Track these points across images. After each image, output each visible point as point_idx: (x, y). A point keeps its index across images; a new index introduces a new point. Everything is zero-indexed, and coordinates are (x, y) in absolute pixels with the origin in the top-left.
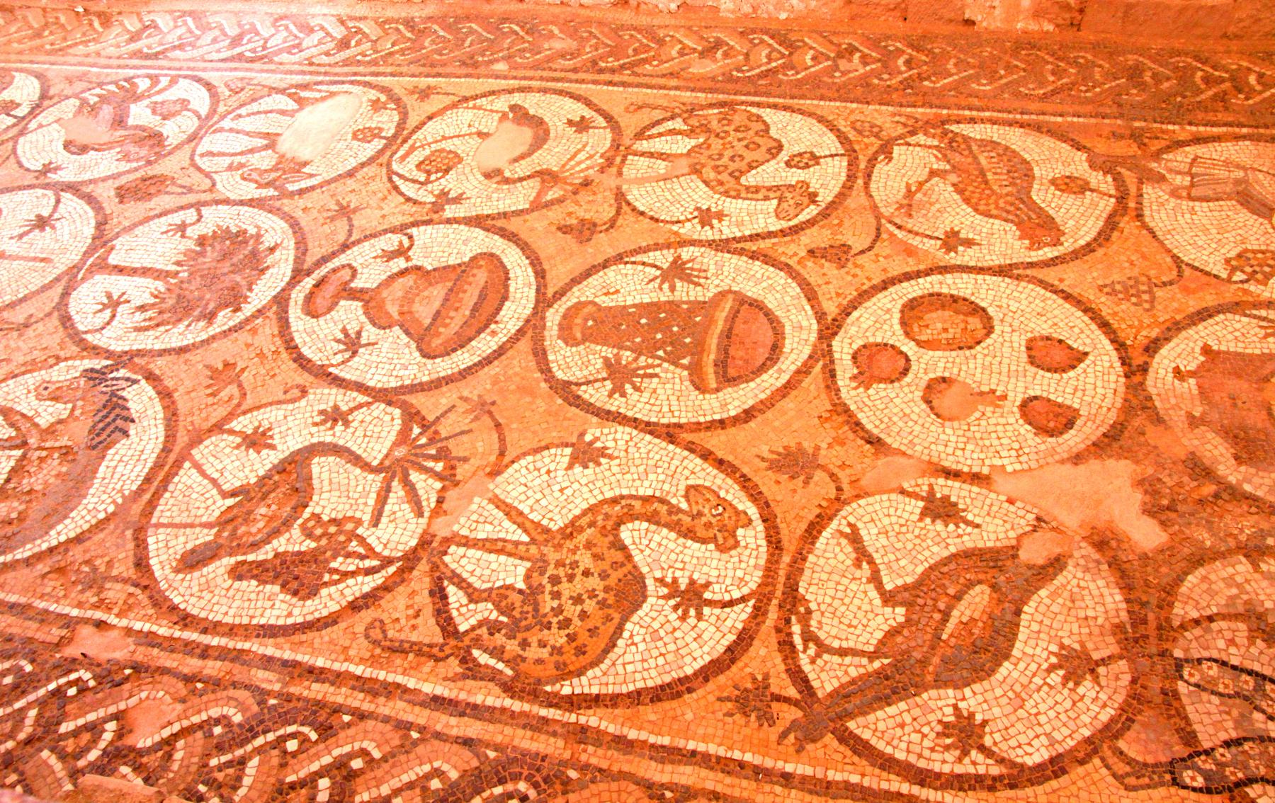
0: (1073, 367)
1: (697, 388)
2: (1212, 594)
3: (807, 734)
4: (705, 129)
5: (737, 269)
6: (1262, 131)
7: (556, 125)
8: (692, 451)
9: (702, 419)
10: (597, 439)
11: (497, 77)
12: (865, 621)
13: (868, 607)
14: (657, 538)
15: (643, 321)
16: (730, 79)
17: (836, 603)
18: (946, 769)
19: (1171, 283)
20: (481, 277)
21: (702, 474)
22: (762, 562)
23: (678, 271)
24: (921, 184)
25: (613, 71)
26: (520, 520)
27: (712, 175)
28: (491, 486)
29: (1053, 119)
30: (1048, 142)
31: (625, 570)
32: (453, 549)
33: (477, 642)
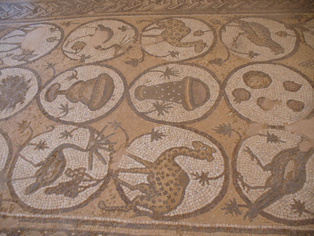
1: (186, 109)
8: (191, 130)
9: (191, 119)
10: (158, 130)
12: (260, 177)
15: (162, 90)
17: (249, 173)
21: (196, 137)
22: (223, 163)
26: (140, 161)
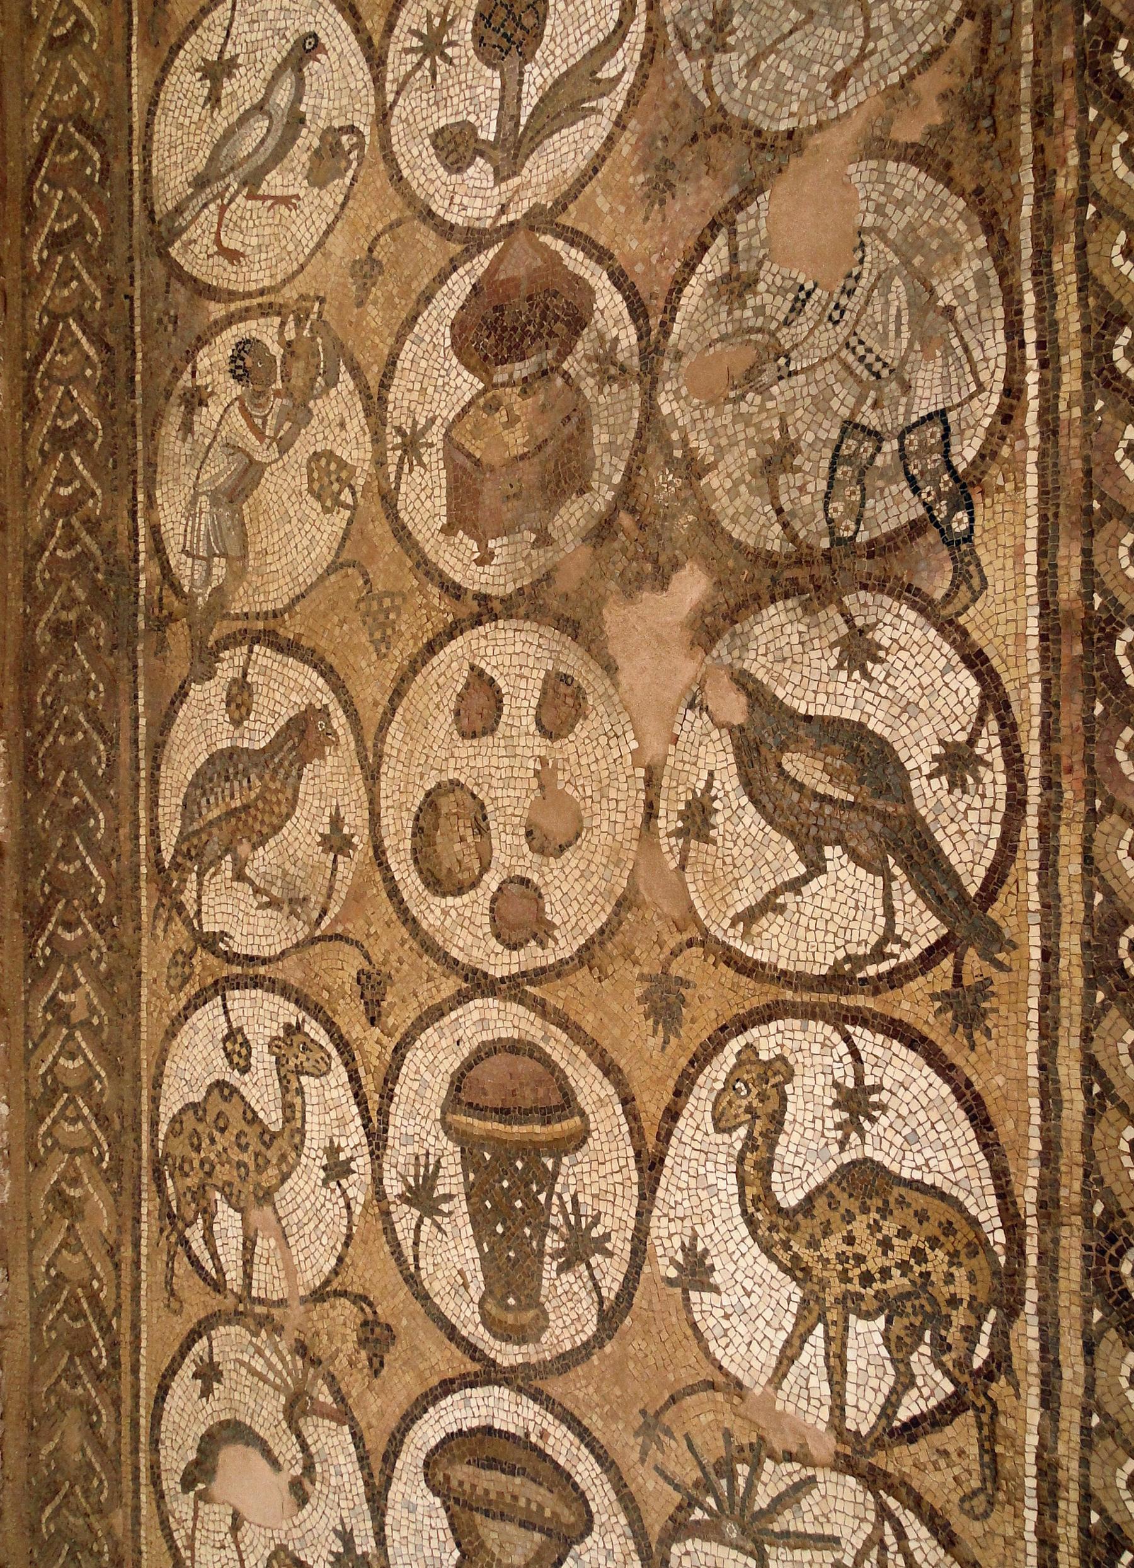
0: (492, 681)
1: (584, 1141)
2: (749, 512)
3: (993, 940)
4: (199, 1193)
5: (409, 1116)
6: (140, 478)
7: (213, 1411)
8: (669, 1134)
9: (625, 1128)
10: (672, 1261)
11: (137, 1522)
12: (849, 891)
13: (831, 889)
14: (789, 1158)
16: (116, 1170)
17: (832, 927)
18: (1002, 778)
19: (365, 574)
20: (462, 1473)
21: (698, 1116)
22: (797, 1023)
23: (423, 1196)
24: (257, 891)
25: (113, 1346)
26: (796, 1342)
27: (272, 1171)
28: (758, 1391)
29: (142, 730)
30: (178, 732)
31: (837, 1192)
32: (850, 1425)
33: (963, 1364)
